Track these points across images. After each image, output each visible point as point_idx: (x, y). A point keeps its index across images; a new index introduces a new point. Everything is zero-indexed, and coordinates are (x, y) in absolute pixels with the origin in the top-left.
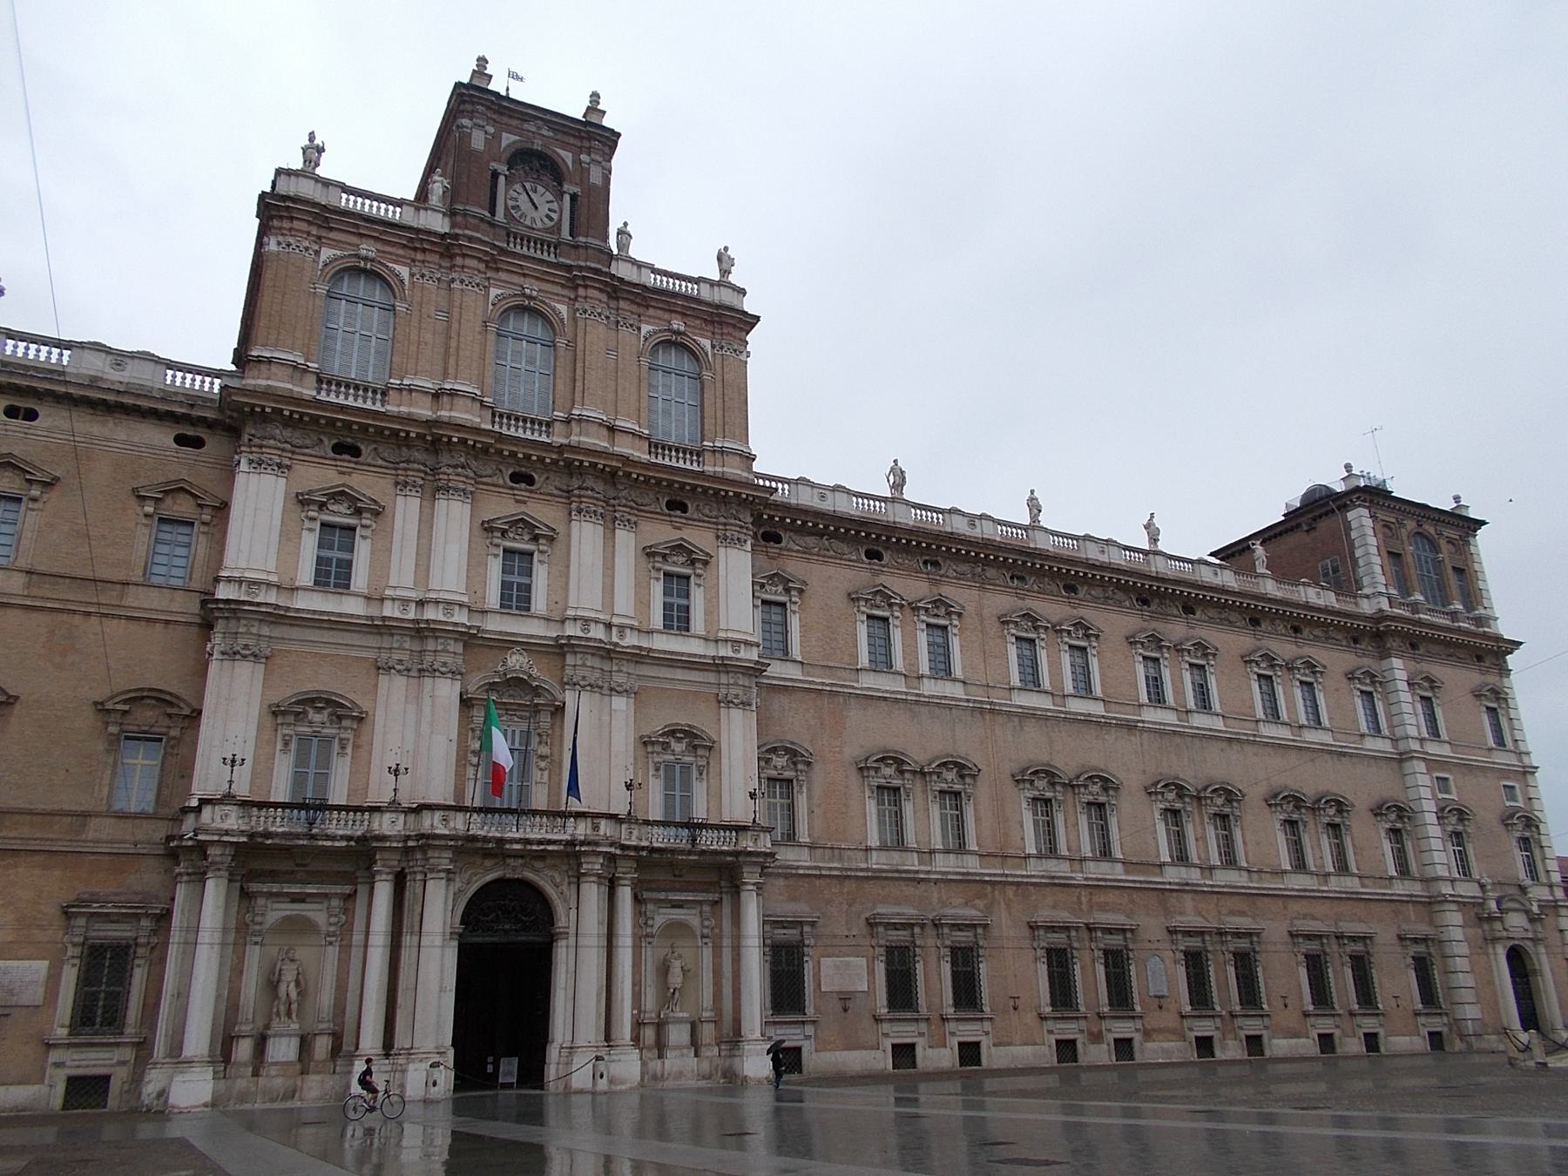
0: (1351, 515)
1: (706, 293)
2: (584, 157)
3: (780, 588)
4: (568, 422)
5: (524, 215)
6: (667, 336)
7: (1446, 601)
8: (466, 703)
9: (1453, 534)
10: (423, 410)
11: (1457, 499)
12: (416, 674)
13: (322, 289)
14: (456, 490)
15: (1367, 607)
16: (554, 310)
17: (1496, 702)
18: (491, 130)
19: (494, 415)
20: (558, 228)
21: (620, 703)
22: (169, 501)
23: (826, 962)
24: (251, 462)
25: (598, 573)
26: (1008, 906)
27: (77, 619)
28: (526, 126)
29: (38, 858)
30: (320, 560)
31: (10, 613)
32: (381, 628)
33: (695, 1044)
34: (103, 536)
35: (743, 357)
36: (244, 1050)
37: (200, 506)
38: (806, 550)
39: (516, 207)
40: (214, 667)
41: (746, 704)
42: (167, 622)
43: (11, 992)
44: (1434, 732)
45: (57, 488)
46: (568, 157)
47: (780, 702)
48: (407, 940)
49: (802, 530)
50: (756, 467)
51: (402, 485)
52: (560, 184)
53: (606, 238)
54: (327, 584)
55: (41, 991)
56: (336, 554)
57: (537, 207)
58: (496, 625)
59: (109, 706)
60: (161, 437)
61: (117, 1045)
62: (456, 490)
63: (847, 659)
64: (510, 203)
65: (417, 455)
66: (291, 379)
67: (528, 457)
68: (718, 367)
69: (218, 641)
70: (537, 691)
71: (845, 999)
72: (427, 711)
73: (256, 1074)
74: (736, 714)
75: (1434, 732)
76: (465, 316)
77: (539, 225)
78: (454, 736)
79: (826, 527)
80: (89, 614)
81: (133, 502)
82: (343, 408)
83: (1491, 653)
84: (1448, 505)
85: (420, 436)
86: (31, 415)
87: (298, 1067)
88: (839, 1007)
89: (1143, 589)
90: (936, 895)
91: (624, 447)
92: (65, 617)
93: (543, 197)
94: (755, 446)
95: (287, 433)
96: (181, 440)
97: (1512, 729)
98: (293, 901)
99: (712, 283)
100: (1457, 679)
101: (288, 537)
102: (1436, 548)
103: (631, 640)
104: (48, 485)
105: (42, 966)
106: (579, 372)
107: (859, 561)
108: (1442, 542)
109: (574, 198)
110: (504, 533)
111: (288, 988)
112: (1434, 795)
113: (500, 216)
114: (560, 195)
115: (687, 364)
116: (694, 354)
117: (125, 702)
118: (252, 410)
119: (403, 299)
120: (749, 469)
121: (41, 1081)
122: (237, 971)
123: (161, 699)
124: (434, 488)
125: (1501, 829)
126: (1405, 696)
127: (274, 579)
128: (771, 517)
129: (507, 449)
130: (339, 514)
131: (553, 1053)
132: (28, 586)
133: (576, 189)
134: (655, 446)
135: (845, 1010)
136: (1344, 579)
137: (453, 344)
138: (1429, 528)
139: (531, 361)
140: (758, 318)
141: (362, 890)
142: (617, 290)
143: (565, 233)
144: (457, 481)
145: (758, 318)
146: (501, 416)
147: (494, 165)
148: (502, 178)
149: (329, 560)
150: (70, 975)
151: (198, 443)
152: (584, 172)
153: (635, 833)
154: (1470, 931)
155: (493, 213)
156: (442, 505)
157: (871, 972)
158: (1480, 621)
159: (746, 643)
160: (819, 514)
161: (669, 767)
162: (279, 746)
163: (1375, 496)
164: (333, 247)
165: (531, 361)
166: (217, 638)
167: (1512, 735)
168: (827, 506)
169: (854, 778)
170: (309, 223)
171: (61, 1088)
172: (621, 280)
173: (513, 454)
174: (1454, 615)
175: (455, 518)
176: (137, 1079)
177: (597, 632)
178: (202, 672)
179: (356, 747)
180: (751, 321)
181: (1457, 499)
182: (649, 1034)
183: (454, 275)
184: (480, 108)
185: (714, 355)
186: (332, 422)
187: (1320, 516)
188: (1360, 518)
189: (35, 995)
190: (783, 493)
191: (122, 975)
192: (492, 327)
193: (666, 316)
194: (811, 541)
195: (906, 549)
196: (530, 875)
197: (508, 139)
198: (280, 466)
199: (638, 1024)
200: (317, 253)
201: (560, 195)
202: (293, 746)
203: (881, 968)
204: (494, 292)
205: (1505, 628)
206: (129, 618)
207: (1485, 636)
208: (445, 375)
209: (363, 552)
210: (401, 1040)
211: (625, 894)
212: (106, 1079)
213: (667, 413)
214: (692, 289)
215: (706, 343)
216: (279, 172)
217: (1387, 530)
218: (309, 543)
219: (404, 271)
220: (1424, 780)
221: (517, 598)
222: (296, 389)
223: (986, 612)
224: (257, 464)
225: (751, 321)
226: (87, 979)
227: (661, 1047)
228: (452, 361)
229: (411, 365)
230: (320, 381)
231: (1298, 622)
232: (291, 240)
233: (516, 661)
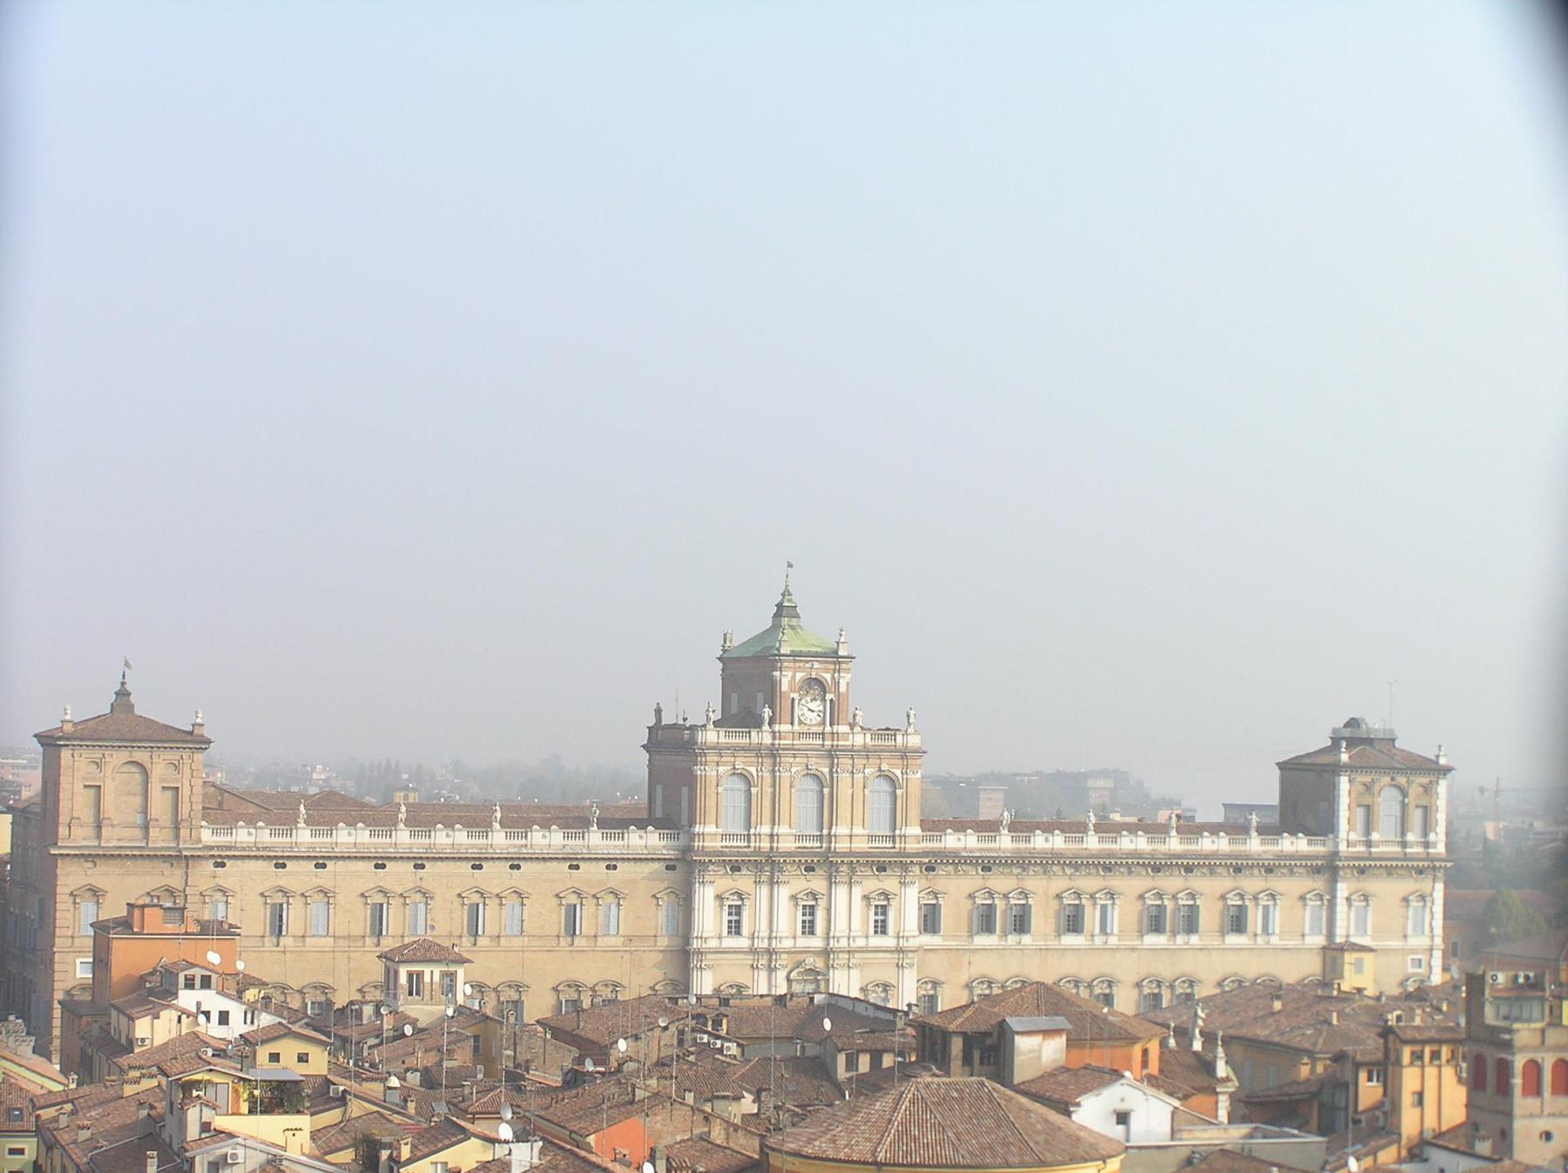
10: (765, 845)
20: (823, 723)
32: (753, 951)
38: (949, 874)
46: (828, 676)
60: (662, 865)
69: (694, 962)
70: (818, 973)
86: (615, 867)
103: (861, 943)
113: (796, 727)
124: (772, 883)
143: (828, 729)
175: (783, 893)
177: (844, 943)
194: (950, 868)
197: (799, 676)
209: (745, 914)
233: (810, 961)
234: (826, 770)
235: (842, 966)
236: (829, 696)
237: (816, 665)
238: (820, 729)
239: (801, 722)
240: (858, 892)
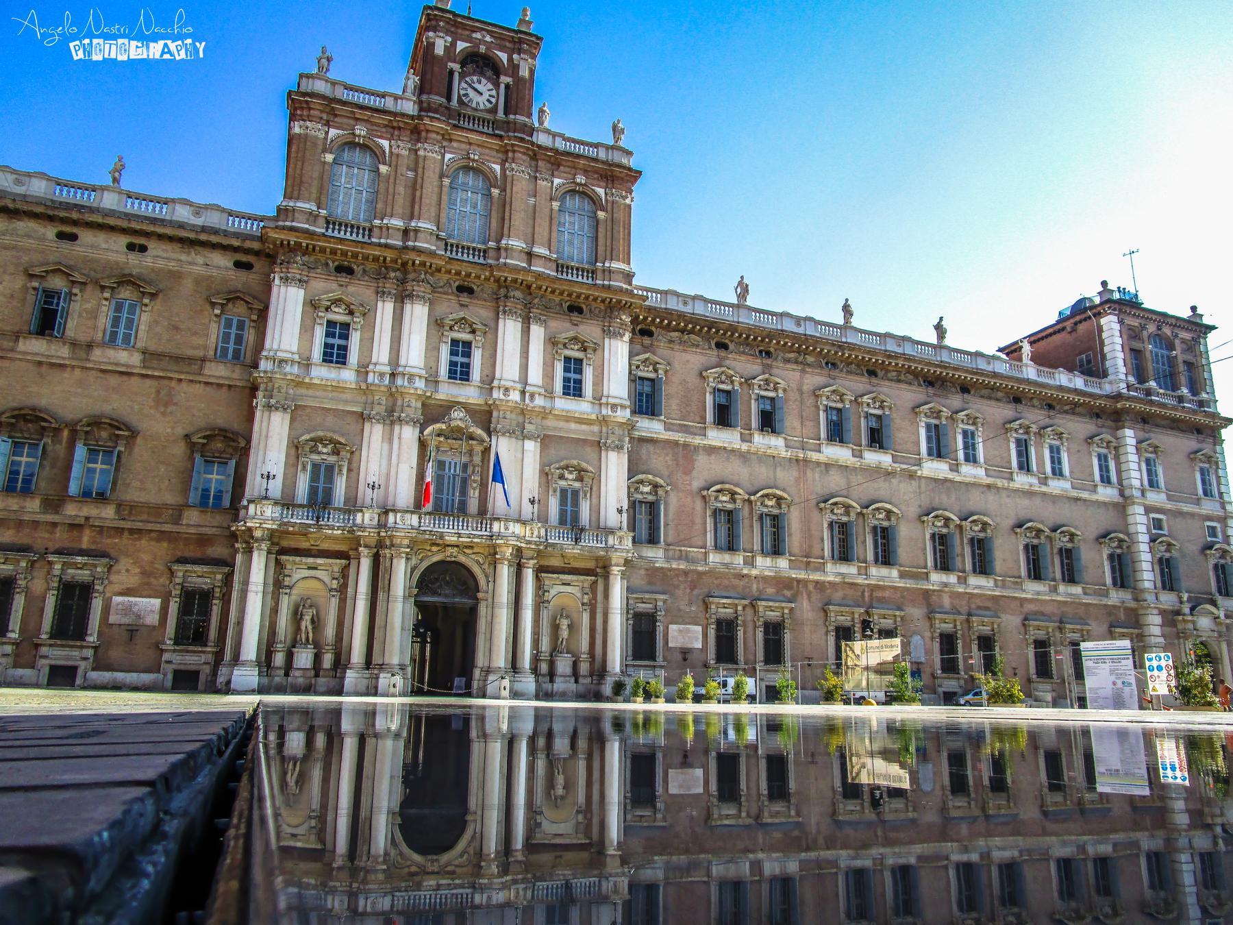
0: (1103, 321)
1: (602, 155)
2: (515, 56)
3: (651, 368)
4: (498, 249)
5: (471, 101)
6: (572, 187)
7: (1175, 387)
8: (422, 444)
9: (1186, 336)
11: (1194, 309)
12: (388, 422)
13: (329, 158)
14: (418, 296)
15: (1108, 389)
16: (491, 169)
17: (1211, 464)
18: (449, 39)
19: (446, 244)
20: (494, 110)
21: (531, 446)
22: (230, 305)
23: (673, 628)
24: (281, 278)
25: (518, 354)
26: (809, 597)
27: (173, 384)
28: (474, 35)
29: (153, 535)
30: (326, 345)
31: (134, 380)
33: (575, 674)
34: (189, 329)
35: (628, 201)
36: (279, 659)
37: (251, 309)
39: (466, 95)
40: (258, 414)
41: (619, 448)
42: (230, 386)
43: (139, 616)
44: (1153, 484)
45: (161, 296)
46: (504, 57)
47: (645, 450)
48: (381, 595)
49: (668, 328)
50: (635, 282)
51: (381, 294)
52: (498, 77)
53: (530, 115)
54: (331, 362)
55: (157, 617)
56: (337, 341)
57: (481, 94)
58: (447, 391)
59: (195, 439)
60: (222, 261)
61: (204, 652)
62: (418, 296)
63: (698, 419)
64: (462, 92)
65: (392, 275)
66: (307, 222)
67: (468, 275)
68: (609, 208)
71: (685, 653)
72: (395, 445)
73: (287, 674)
74: (613, 455)
75: (1153, 484)
76: (427, 174)
77: (482, 107)
78: (415, 465)
79: (686, 326)
80: (180, 380)
81: (208, 307)
82: (341, 240)
83: (1206, 429)
84: (1186, 314)
85: (395, 261)
86: (143, 249)
87: (313, 672)
88: (679, 657)
89: (942, 377)
90: (755, 586)
91: (538, 268)
92: (166, 382)
93: (485, 86)
94: (634, 266)
95: (306, 258)
96: (238, 265)
97: (1219, 484)
98: (309, 568)
99: (608, 148)
100: (1177, 444)
101: (306, 330)
102: (1171, 347)
103: (539, 401)
104: (153, 296)
105: (157, 602)
106: (507, 214)
107: (710, 348)
108: (1177, 342)
109: (507, 86)
110: (451, 328)
111: (306, 623)
112: (1149, 531)
114: (497, 85)
115: (587, 205)
116: (594, 200)
117: (204, 437)
118: (282, 244)
119: (384, 163)
120: (630, 284)
121: (158, 672)
122: (275, 611)
123: (225, 434)
124: (402, 298)
125: (1201, 558)
126: (1133, 458)
127: (296, 357)
128: (645, 318)
129: (454, 267)
130: (339, 315)
131: (477, 673)
132: (144, 361)
133: (509, 80)
134: (560, 267)
135: (685, 660)
136: (1094, 367)
137: (418, 194)
138: (1167, 331)
139: (475, 206)
140: (640, 173)
141: (354, 563)
142: (536, 154)
143: (501, 114)
144: (419, 289)
145: (640, 173)
146: (452, 245)
147: (451, 65)
148: (456, 76)
149: (332, 346)
150: (174, 607)
151: (247, 266)
152: (515, 68)
153: (536, 533)
154: (1167, 629)
155: (449, 99)
156: (408, 307)
157: (705, 635)
158: (1201, 404)
159: (623, 407)
160: (681, 316)
161: (564, 492)
162: (300, 467)
163: (1126, 305)
164: (338, 128)
165: (475, 206)
166: (260, 394)
167: (1219, 489)
168: (688, 309)
169: (699, 504)
170: (322, 111)
171: (170, 676)
172: (539, 147)
173: (458, 273)
174: (1181, 399)
175: (418, 315)
176: (215, 673)
178: (250, 419)
179: (349, 470)
180: (634, 176)
181: (1194, 309)
182: (544, 667)
183: (419, 145)
184: (442, 24)
185: (607, 200)
186: (334, 252)
187: (1080, 322)
188: (1110, 324)
189: (153, 619)
190: (654, 301)
191: (206, 612)
192: (446, 181)
193: (573, 171)
195: (746, 342)
196: (462, 559)
197: (461, 45)
198: (300, 281)
199: (536, 659)
200: (327, 133)
201: (497, 85)
202: (309, 468)
203: (712, 633)
204: (448, 156)
205: (1225, 408)
206: (206, 383)
207: (1207, 414)
208: (412, 218)
209: (355, 338)
210: (376, 659)
211: (529, 575)
212: (198, 672)
213: (571, 243)
214: (592, 152)
215: (601, 191)
216: (301, 76)
217: (1132, 335)
218: (320, 332)
219: (385, 143)
220: (1143, 519)
221: (460, 372)
222: (312, 228)
223: (805, 388)
224: (285, 280)
225: (634, 176)
226: (185, 610)
227: (552, 675)
228: (417, 207)
229: (389, 210)
230: (328, 222)
231: (1052, 404)
232: (308, 123)
233: (458, 417)
234: (497, 168)
235: (510, 433)
236: (505, 79)
237: (488, 39)
238: (488, 116)
239: (460, 102)
240: (537, 333)
